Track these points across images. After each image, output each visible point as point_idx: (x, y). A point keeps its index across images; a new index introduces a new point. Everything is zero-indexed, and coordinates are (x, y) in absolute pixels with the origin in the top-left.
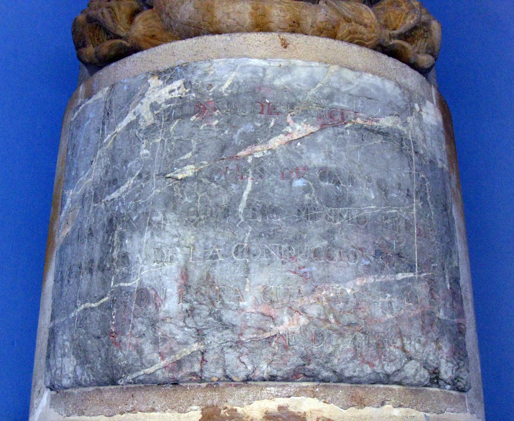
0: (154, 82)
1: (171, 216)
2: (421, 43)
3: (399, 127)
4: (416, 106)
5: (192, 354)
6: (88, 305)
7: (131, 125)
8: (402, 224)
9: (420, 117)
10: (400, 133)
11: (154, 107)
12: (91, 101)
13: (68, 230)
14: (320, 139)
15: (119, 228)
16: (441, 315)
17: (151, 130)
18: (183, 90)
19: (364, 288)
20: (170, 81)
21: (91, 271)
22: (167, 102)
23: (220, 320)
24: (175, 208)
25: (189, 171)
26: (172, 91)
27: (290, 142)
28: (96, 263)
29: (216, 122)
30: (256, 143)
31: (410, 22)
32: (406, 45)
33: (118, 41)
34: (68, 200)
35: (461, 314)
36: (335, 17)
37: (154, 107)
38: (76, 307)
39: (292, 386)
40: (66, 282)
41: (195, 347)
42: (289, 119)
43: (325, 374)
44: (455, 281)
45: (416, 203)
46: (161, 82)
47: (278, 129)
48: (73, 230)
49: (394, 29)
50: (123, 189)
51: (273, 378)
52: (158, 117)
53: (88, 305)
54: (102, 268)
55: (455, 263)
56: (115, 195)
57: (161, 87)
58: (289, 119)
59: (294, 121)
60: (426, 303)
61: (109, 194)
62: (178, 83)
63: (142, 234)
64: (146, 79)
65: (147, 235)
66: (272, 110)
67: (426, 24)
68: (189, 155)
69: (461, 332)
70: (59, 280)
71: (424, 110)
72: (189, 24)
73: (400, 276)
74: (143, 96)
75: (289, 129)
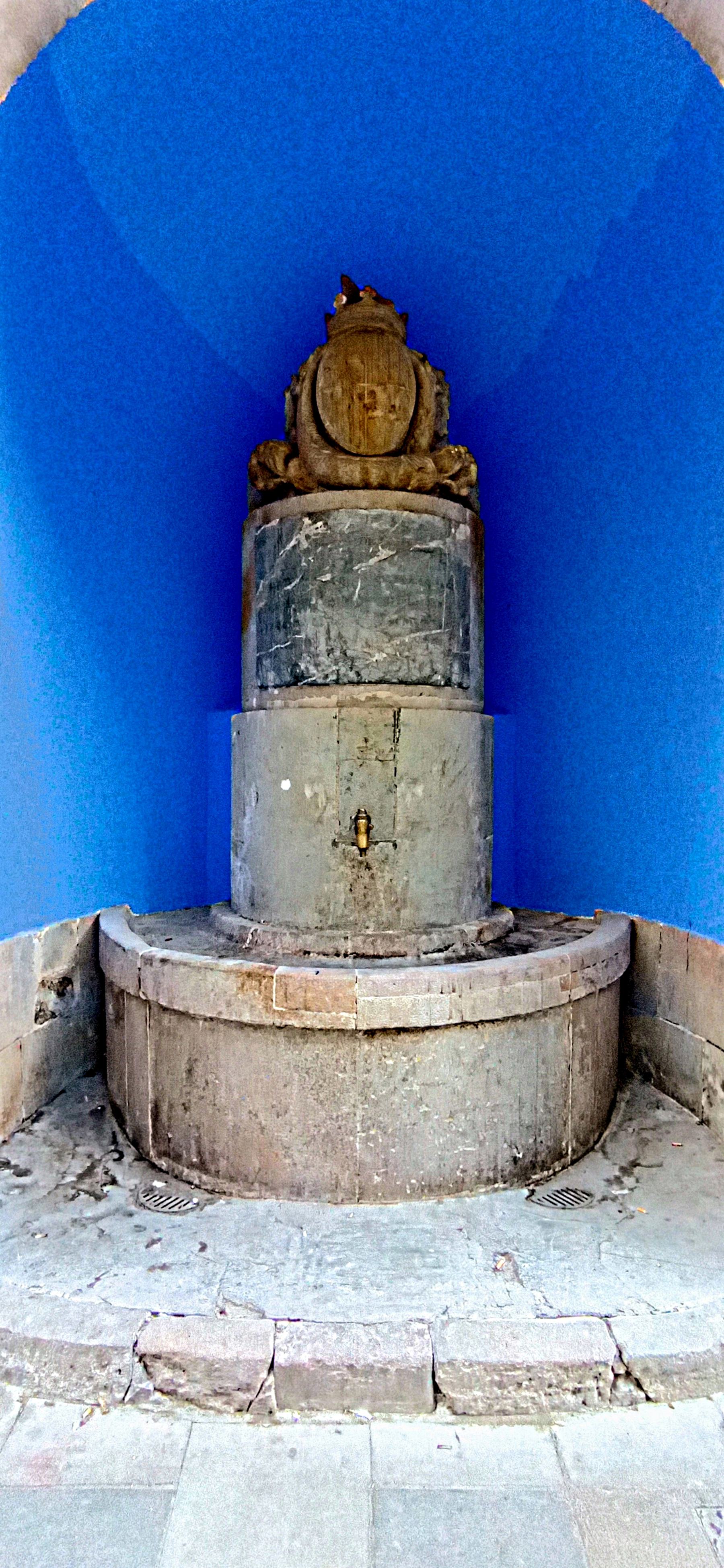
0: (307, 521)
1: (320, 602)
2: (463, 480)
3: (441, 546)
4: (453, 530)
5: (333, 671)
6: (279, 646)
7: (294, 547)
8: (437, 604)
9: (454, 537)
10: (440, 549)
11: (307, 537)
12: (269, 525)
13: (263, 603)
14: (396, 557)
15: (293, 606)
16: (455, 651)
17: (307, 551)
18: (323, 528)
19: (415, 639)
20: (315, 522)
21: (279, 628)
22: (315, 535)
23: (345, 654)
24: (322, 597)
25: (328, 577)
26: (317, 528)
27: (380, 561)
28: (282, 624)
29: (341, 549)
30: (363, 562)
31: (457, 467)
32: (453, 483)
33: (278, 480)
34: (261, 586)
35: (468, 649)
36: (410, 469)
37: (307, 537)
38: (272, 647)
39: (380, 686)
40: (264, 632)
41: (334, 668)
42: (380, 548)
43: (395, 680)
44: (466, 632)
45: (447, 590)
46: (310, 522)
47: (374, 554)
48: (266, 605)
49: (446, 472)
50: (293, 584)
51: (370, 682)
52: (310, 544)
53: (279, 646)
54: (285, 627)
55: (467, 622)
56: (289, 587)
57: (310, 525)
58: (380, 548)
59: (383, 547)
60: (447, 644)
61: (286, 586)
62: (320, 524)
63: (305, 611)
64: (301, 519)
65: (309, 610)
66: (370, 542)
67: (468, 467)
68: (328, 568)
69: (467, 658)
70: (259, 631)
71: (458, 531)
72: (323, 476)
73: (433, 632)
74: (301, 529)
75: (379, 553)
